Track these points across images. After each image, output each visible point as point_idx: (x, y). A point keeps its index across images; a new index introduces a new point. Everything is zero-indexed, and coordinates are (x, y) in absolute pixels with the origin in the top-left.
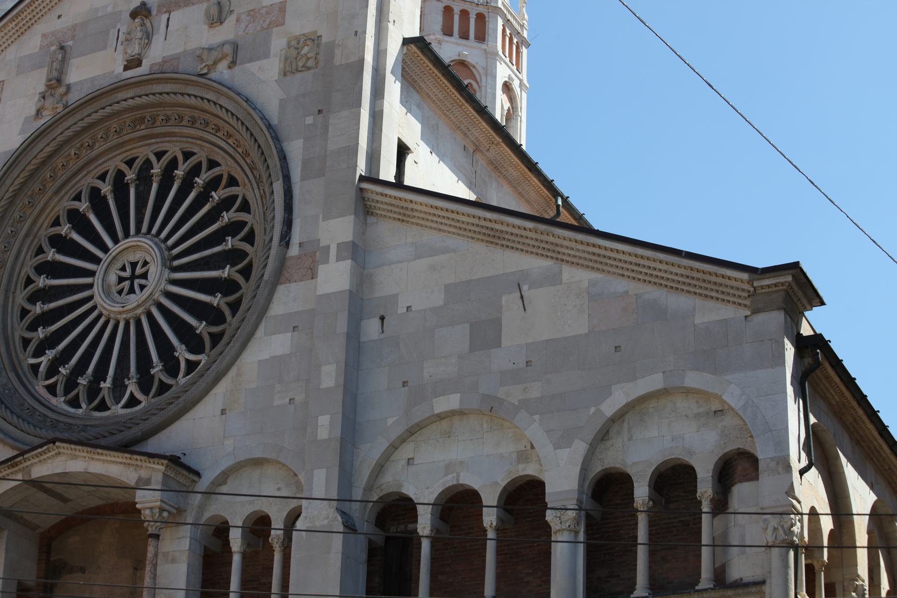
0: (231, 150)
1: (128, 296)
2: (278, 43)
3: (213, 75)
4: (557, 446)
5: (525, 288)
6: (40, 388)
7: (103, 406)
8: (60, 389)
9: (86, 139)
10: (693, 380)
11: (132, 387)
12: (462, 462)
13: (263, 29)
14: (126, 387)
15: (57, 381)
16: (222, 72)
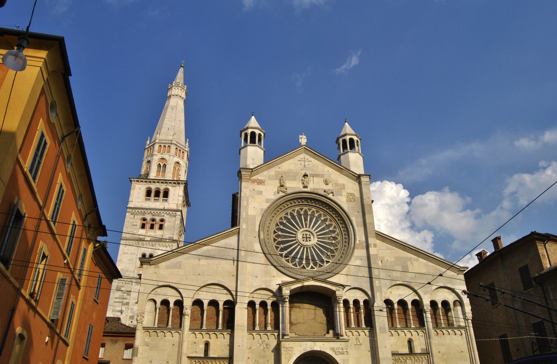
0: (332, 214)
1: (306, 242)
2: (344, 193)
3: (328, 196)
4: (424, 295)
5: (412, 261)
6: (284, 260)
7: (304, 267)
8: (290, 261)
9: (292, 202)
10: (449, 285)
11: (311, 264)
12: (402, 295)
13: (339, 189)
14: (309, 264)
15: (289, 259)
16: (330, 196)
